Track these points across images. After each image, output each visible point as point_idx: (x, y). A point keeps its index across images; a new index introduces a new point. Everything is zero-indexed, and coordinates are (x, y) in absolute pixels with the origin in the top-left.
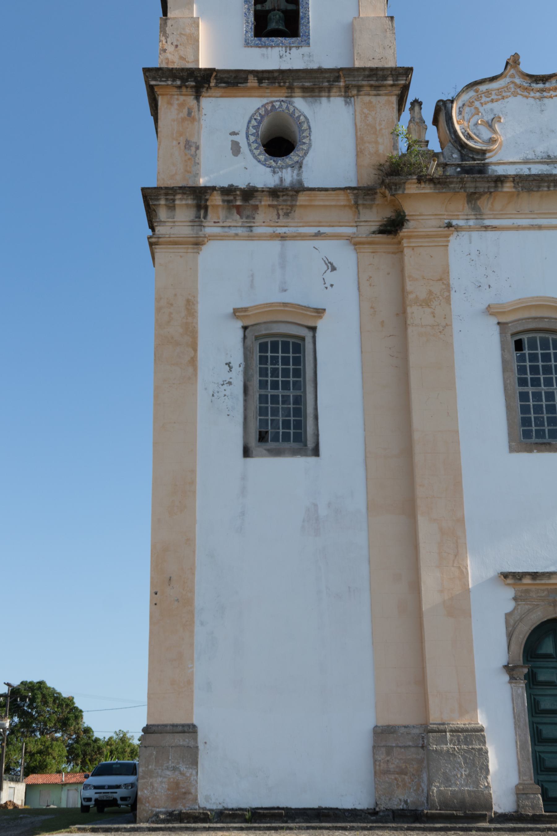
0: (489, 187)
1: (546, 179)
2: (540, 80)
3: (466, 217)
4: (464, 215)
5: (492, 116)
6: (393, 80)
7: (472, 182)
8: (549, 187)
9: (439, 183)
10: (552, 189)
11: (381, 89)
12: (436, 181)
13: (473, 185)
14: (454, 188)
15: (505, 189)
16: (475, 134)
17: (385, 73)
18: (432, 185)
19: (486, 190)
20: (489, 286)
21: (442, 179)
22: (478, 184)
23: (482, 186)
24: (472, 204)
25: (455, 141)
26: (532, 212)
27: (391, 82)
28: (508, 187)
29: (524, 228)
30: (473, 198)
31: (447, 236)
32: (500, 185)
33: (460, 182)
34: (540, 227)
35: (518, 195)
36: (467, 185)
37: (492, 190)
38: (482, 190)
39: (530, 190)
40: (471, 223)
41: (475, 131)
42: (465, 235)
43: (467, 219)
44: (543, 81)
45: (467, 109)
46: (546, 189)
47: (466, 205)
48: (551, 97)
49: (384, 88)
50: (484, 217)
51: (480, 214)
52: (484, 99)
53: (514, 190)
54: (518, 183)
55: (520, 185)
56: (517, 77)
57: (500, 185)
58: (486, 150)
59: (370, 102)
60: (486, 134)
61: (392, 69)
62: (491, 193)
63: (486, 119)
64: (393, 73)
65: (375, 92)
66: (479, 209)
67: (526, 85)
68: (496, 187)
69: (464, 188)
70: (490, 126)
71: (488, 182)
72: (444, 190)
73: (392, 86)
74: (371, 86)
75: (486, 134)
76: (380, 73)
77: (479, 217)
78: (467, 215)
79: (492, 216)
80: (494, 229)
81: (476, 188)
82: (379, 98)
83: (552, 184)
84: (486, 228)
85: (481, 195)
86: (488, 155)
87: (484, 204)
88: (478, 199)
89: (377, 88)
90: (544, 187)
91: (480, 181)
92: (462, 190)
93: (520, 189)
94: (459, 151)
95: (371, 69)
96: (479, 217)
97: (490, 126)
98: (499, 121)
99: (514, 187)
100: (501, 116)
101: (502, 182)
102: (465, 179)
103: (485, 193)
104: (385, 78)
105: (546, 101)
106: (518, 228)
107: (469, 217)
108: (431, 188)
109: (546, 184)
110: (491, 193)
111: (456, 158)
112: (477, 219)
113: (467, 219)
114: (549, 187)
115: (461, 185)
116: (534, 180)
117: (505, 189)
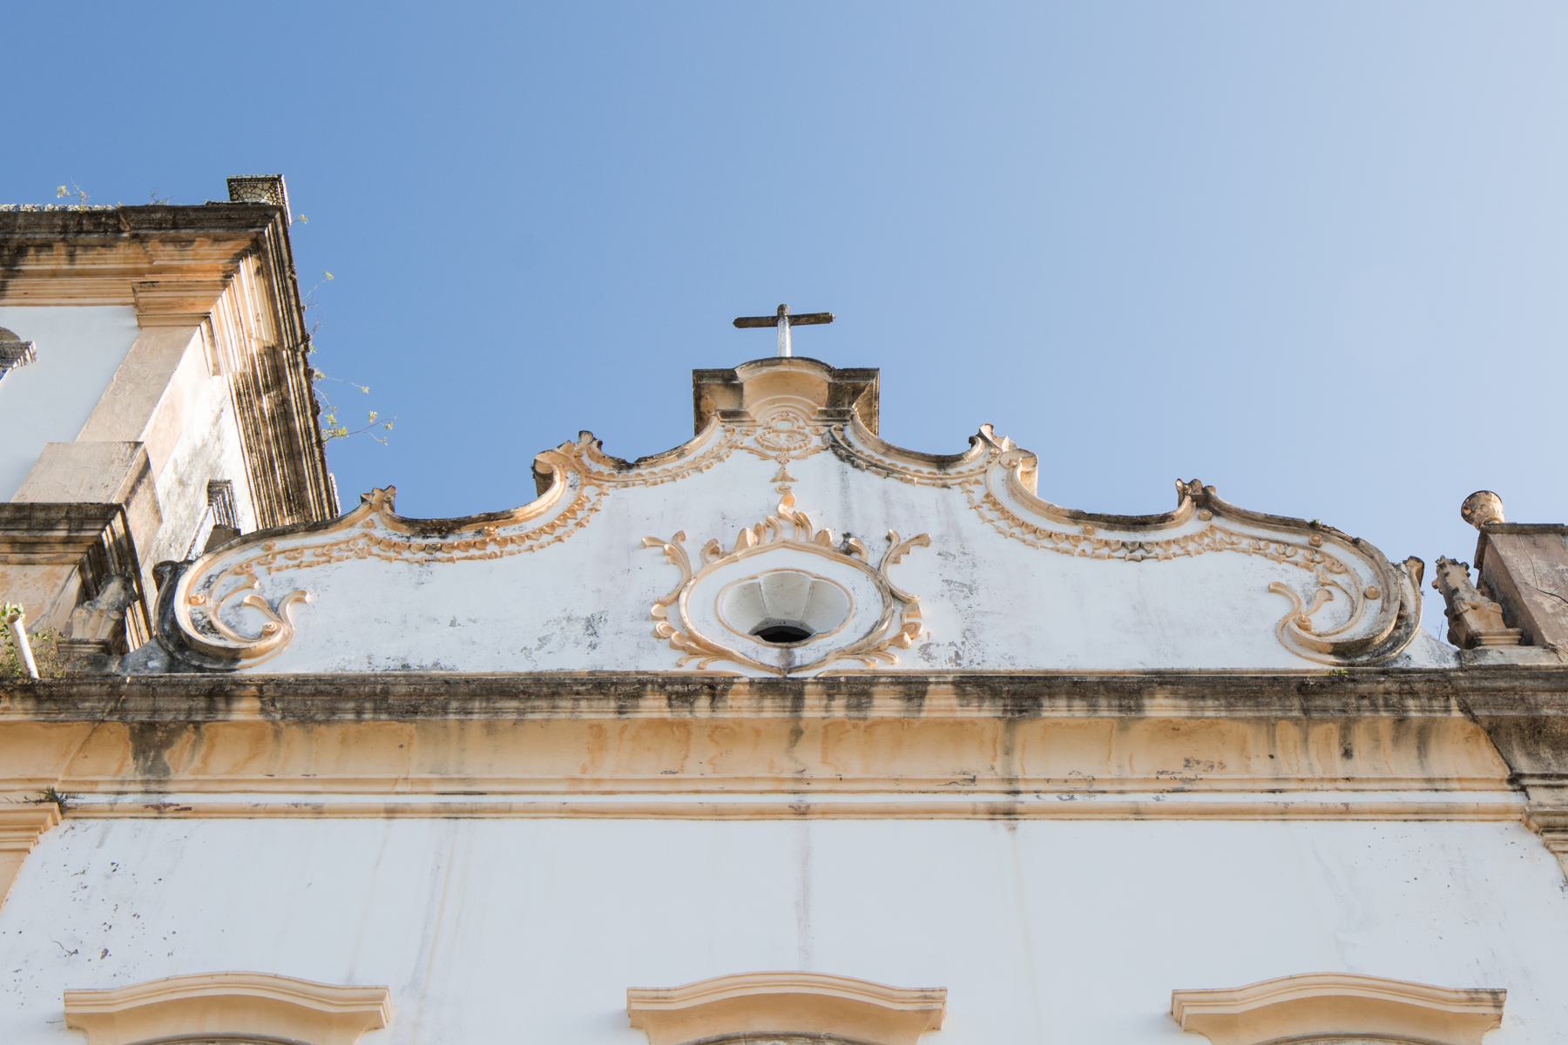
0: (190, 711)
1: (352, 690)
2: (433, 531)
3: (117, 788)
4: (112, 782)
5: (287, 591)
6: (69, 530)
7: (144, 695)
8: (359, 712)
9: (50, 697)
10: (367, 716)
11: (38, 548)
12: (41, 691)
13: (145, 704)
14: (92, 711)
15: (235, 717)
16: (227, 623)
17: (53, 514)
18: (30, 704)
19: (182, 718)
20: (106, 952)
21: (58, 685)
22: (162, 703)
23: (172, 709)
24: (146, 759)
25: (168, 637)
26: (307, 778)
27: (63, 534)
28: (245, 710)
29: (272, 812)
30: (149, 740)
31: (35, 827)
32: (221, 705)
33: (109, 695)
34: (318, 812)
35: (277, 734)
36: (130, 705)
37: (199, 718)
38: (169, 717)
39: (305, 720)
40: (127, 800)
41: (230, 618)
42: (95, 826)
43: (119, 793)
44: (440, 531)
45: (227, 579)
46: (351, 716)
47: (130, 760)
48: (451, 560)
49: (45, 548)
50: (169, 788)
51: (160, 782)
52: (280, 561)
53: (260, 718)
54: (273, 700)
55: (278, 705)
56: (380, 526)
57: (221, 705)
58: (237, 650)
59: (4, 575)
60: (255, 621)
61: (70, 507)
62: (197, 725)
63: (268, 596)
64: (73, 515)
65: (21, 556)
66: (166, 771)
67: (395, 539)
68: (211, 709)
69: (120, 712)
70: (274, 609)
71: (189, 696)
72: (62, 716)
73: (67, 541)
74: (13, 542)
75: (255, 621)
76: (41, 515)
77: (153, 787)
78: (122, 782)
79: (191, 787)
80: (182, 814)
81: (155, 711)
82: (28, 569)
83: (368, 705)
84: (160, 810)
85: (173, 733)
86: (243, 662)
87: (182, 759)
88: (166, 744)
89: (28, 546)
90: (345, 711)
91: (165, 695)
92: (115, 718)
93: (278, 716)
94: (170, 654)
95: (19, 507)
96: (153, 787)
97: (274, 609)
98: (300, 600)
99: (262, 711)
100: (309, 589)
101: (229, 697)
102: (123, 688)
103: (182, 727)
104: (50, 525)
105: (436, 566)
106: (251, 813)
107: (126, 788)
108: (26, 712)
109: (351, 705)
110: (197, 725)
111: (153, 669)
112: (147, 792)
113: (119, 793)
114: (359, 712)
115: (113, 704)
116: (318, 693)
117: (236, 717)
